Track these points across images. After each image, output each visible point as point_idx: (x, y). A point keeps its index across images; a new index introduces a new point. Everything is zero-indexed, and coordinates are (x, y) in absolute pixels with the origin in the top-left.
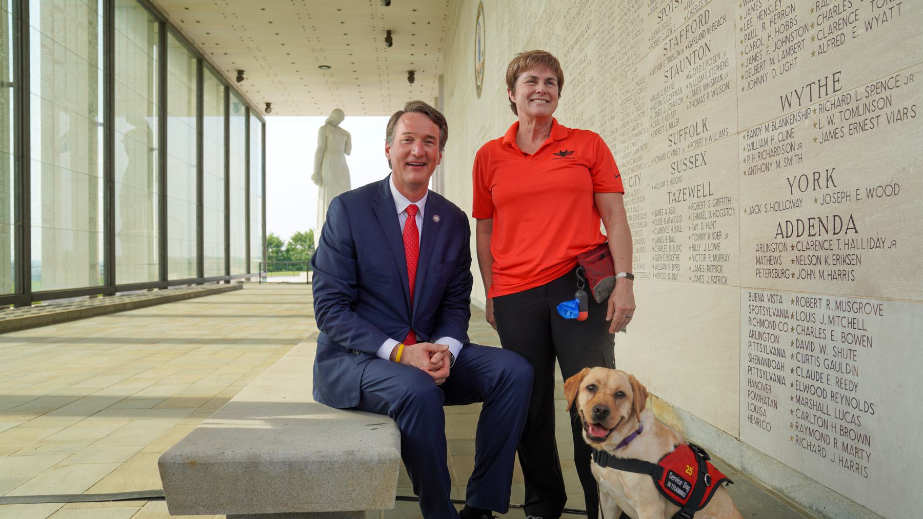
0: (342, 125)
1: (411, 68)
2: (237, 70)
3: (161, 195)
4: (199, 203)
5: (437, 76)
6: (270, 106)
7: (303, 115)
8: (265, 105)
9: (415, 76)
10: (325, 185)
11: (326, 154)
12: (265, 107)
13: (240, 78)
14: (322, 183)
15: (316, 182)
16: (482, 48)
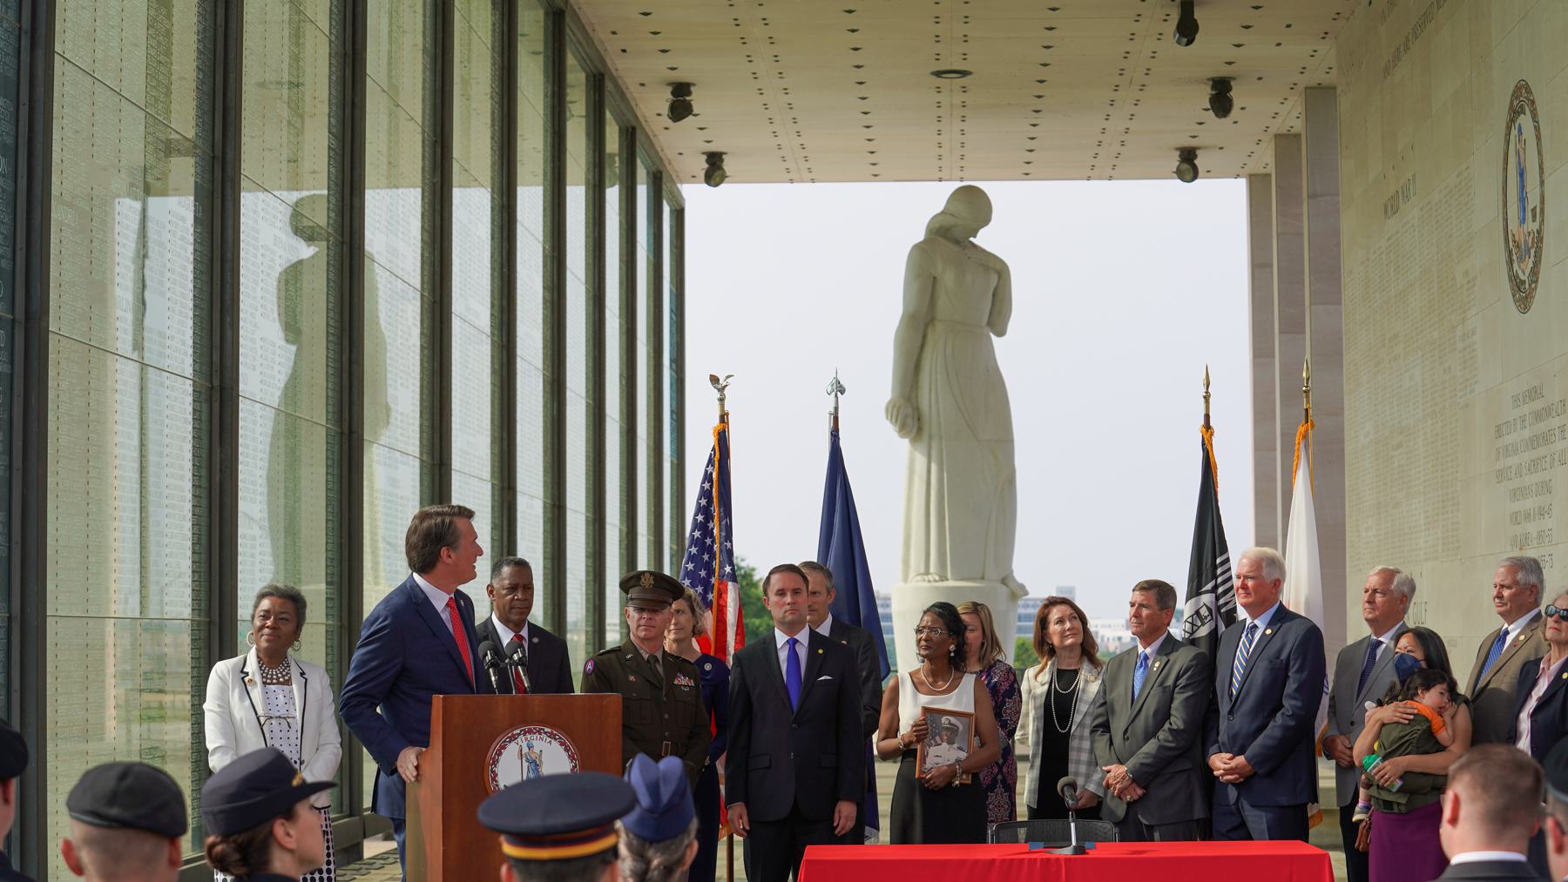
0: (984, 239)
1: (1224, 71)
2: (669, 84)
3: (553, 506)
4: (595, 513)
5: (1300, 87)
6: (722, 161)
7: (813, 181)
8: (705, 157)
9: (1232, 93)
10: (930, 438)
11: (930, 330)
12: (706, 166)
13: (680, 108)
14: (920, 430)
15: (903, 429)
16: (1533, 200)
